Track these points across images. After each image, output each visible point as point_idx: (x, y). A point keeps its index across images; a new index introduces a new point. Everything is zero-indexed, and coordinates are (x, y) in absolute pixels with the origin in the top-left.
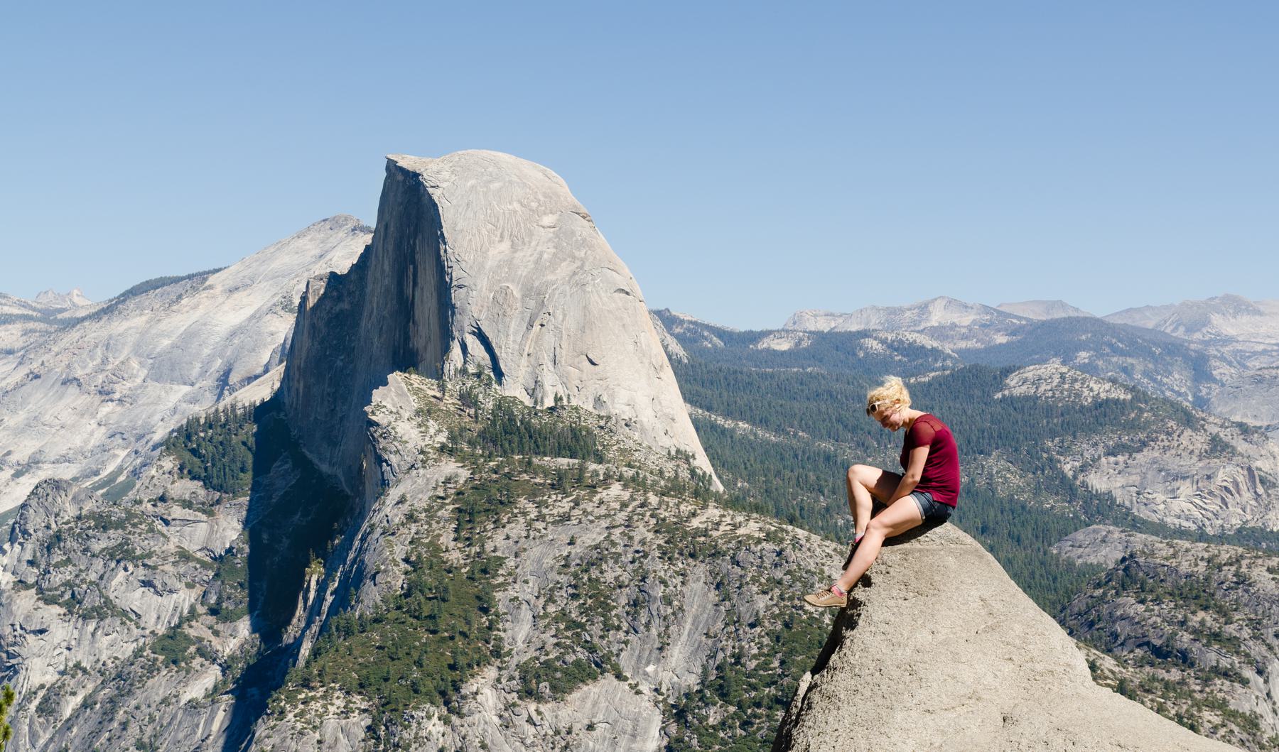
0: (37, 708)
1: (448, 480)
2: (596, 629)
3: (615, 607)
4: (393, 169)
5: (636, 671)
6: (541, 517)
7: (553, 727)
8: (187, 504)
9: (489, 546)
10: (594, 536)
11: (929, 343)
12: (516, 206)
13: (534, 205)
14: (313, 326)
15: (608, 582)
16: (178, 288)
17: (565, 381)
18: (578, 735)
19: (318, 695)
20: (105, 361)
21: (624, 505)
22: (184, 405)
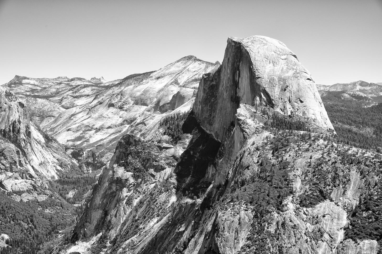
0: (126, 202)
1: (267, 138)
2: (322, 185)
5: (336, 198)
7: (312, 215)
8: (167, 142)
9: (284, 158)
10: (318, 156)
12: (273, 53)
13: (279, 53)
14: (204, 89)
15: (324, 170)
16: (140, 77)
17: (293, 107)
18: (320, 218)
19: (237, 203)
20: (121, 99)
21: (326, 146)
22: (146, 112)
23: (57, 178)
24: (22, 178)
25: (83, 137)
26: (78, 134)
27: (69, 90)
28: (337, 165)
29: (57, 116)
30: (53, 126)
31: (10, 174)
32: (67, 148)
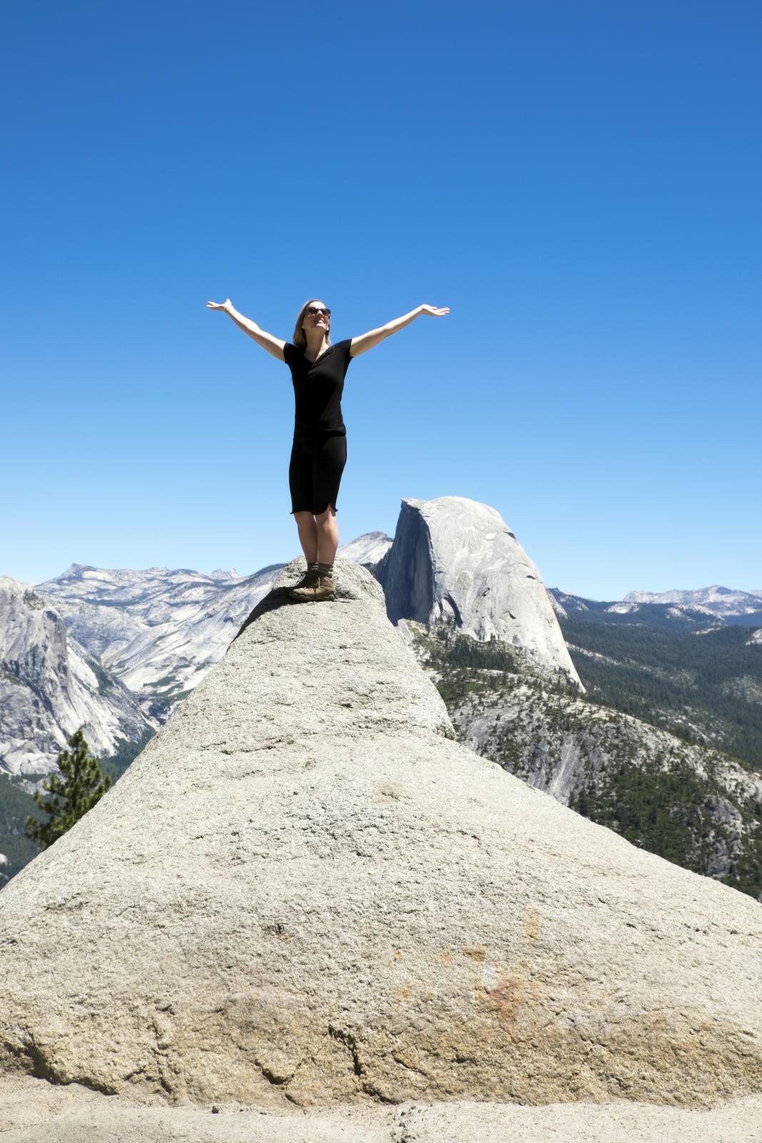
3: (522, 756)
4: (405, 506)
6: (481, 703)
11: (709, 612)
12: (472, 528)
13: (482, 528)
21: (528, 698)
23: (112, 752)
24: (42, 750)
25: (173, 679)
26: (164, 674)
27: (165, 592)
28: (541, 732)
29: (132, 638)
30: (124, 657)
31: (19, 742)
32: (142, 700)
